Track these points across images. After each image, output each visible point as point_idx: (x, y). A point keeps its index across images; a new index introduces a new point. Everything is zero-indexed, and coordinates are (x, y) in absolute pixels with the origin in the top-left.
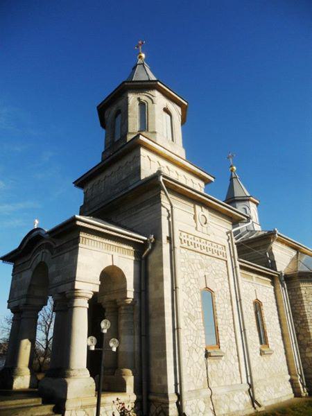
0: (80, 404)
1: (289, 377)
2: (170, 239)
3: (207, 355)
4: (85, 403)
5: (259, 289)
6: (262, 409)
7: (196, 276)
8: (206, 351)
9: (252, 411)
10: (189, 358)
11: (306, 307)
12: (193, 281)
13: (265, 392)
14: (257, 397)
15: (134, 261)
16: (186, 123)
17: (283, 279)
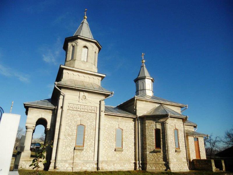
0: (23, 160)
1: (134, 161)
2: (62, 107)
3: (74, 149)
4: (25, 160)
5: (128, 125)
6: (57, 170)
7: (76, 120)
8: (75, 148)
9: (96, 170)
10: (65, 149)
11: (147, 132)
12: (73, 122)
13: (113, 166)
14: (57, 165)
15: (52, 115)
16: (88, 48)
17: (138, 118)
